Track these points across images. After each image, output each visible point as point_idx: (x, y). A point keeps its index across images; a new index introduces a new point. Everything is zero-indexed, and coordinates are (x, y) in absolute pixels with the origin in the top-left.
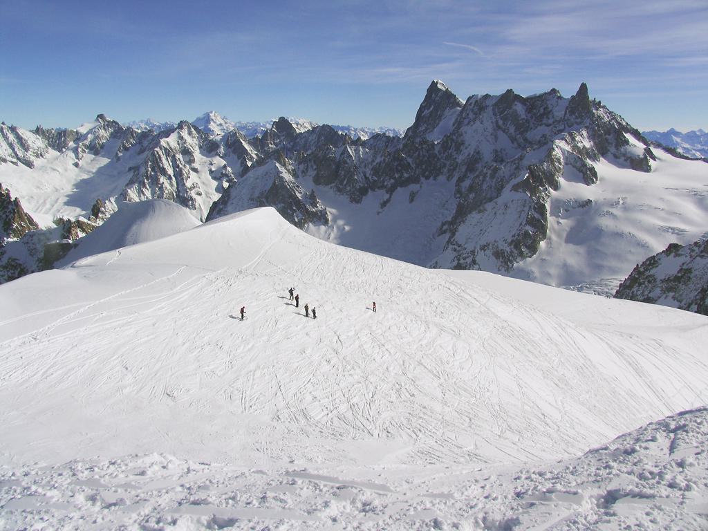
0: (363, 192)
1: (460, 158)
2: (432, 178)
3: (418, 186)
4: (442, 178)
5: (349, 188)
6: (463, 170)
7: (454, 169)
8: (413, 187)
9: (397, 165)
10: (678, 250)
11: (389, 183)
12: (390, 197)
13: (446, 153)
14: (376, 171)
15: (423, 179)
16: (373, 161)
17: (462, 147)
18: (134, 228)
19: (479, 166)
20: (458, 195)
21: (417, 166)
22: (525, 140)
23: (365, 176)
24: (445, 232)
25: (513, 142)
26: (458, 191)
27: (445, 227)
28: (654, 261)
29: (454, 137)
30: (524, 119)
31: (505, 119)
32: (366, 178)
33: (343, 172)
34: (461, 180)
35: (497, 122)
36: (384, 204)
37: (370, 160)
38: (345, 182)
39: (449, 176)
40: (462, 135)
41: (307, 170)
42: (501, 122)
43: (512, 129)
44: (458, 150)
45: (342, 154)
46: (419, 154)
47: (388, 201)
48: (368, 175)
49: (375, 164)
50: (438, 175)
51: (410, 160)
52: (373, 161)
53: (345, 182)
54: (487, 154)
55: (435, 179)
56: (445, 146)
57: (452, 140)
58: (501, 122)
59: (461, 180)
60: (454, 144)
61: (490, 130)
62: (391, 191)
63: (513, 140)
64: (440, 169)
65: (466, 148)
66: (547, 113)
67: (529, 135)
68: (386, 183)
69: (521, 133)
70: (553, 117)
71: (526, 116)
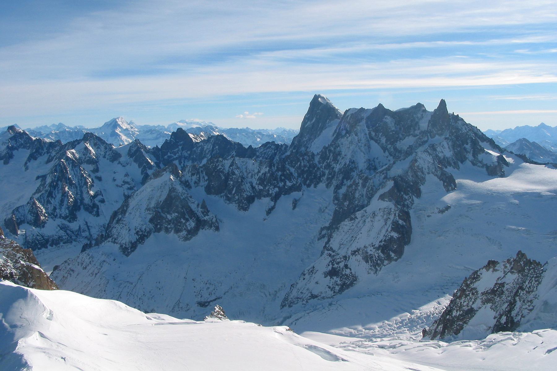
0: (251, 200)
1: (337, 167)
2: (312, 186)
3: (301, 193)
4: (322, 186)
5: (237, 197)
6: (340, 178)
7: (333, 177)
8: (295, 195)
9: (281, 176)
10: (495, 266)
11: (274, 191)
12: (275, 205)
13: (325, 163)
14: (262, 181)
15: (304, 187)
16: (259, 172)
17: (339, 157)
18: (16, 304)
19: (354, 174)
20: (336, 202)
21: (299, 176)
22: (395, 149)
23: (252, 186)
24: (324, 236)
25: (384, 152)
26: (336, 198)
27: (324, 232)
28: (477, 275)
29: (332, 149)
30: (394, 131)
31: (376, 131)
32: (253, 188)
33: (232, 183)
34: (338, 187)
35: (370, 134)
36: (270, 211)
37: (256, 171)
38: (234, 192)
39: (328, 183)
40: (339, 146)
41: (199, 180)
42: (373, 134)
43: (383, 140)
44: (336, 160)
45: (231, 166)
46: (300, 165)
47: (273, 208)
48: (254, 185)
49: (260, 174)
50: (318, 183)
51: (292, 170)
52: (259, 172)
53: (234, 192)
54: (362, 164)
55: (315, 187)
56: (324, 156)
57: (330, 151)
58: (373, 134)
59: (338, 187)
60: (332, 155)
61: (363, 141)
62: (276, 198)
63: (385, 149)
64: (320, 177)
65: (343, 158)
66: (415, 124)
67: (398, 145)
68: (270, 192)
69: (392, 143)
70: (419, 129)
71: (396, 128)
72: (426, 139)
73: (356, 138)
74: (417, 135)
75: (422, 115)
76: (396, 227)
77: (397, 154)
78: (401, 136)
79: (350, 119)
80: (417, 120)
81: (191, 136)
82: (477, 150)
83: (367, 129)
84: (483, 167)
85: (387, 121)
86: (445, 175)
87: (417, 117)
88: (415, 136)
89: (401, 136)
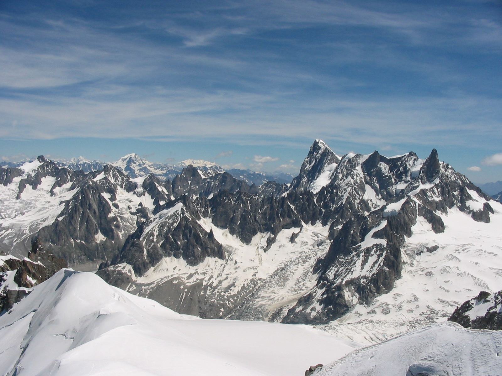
1: (333, 207)
8: (296, 230)
22: (388, 193)
30: (387, 176)
31: (370, 175)
51: (292, 207)
62: (275, 232)
72: (417, 184)
73: (352, 181)
74: (409, 181)
75: (414, 163)
76: (387, 262)
77: (390, 198)
78: (393, 180)
79: (347, 164)
80: (409, 167)
81: (200, 172)
82: (465, 197)
83: (362, 173)
84: (469, 213)
85: (381, 166)
86: (434, 218)
87: (410, 165)
88: (406, 182)
89: (393, 180)
